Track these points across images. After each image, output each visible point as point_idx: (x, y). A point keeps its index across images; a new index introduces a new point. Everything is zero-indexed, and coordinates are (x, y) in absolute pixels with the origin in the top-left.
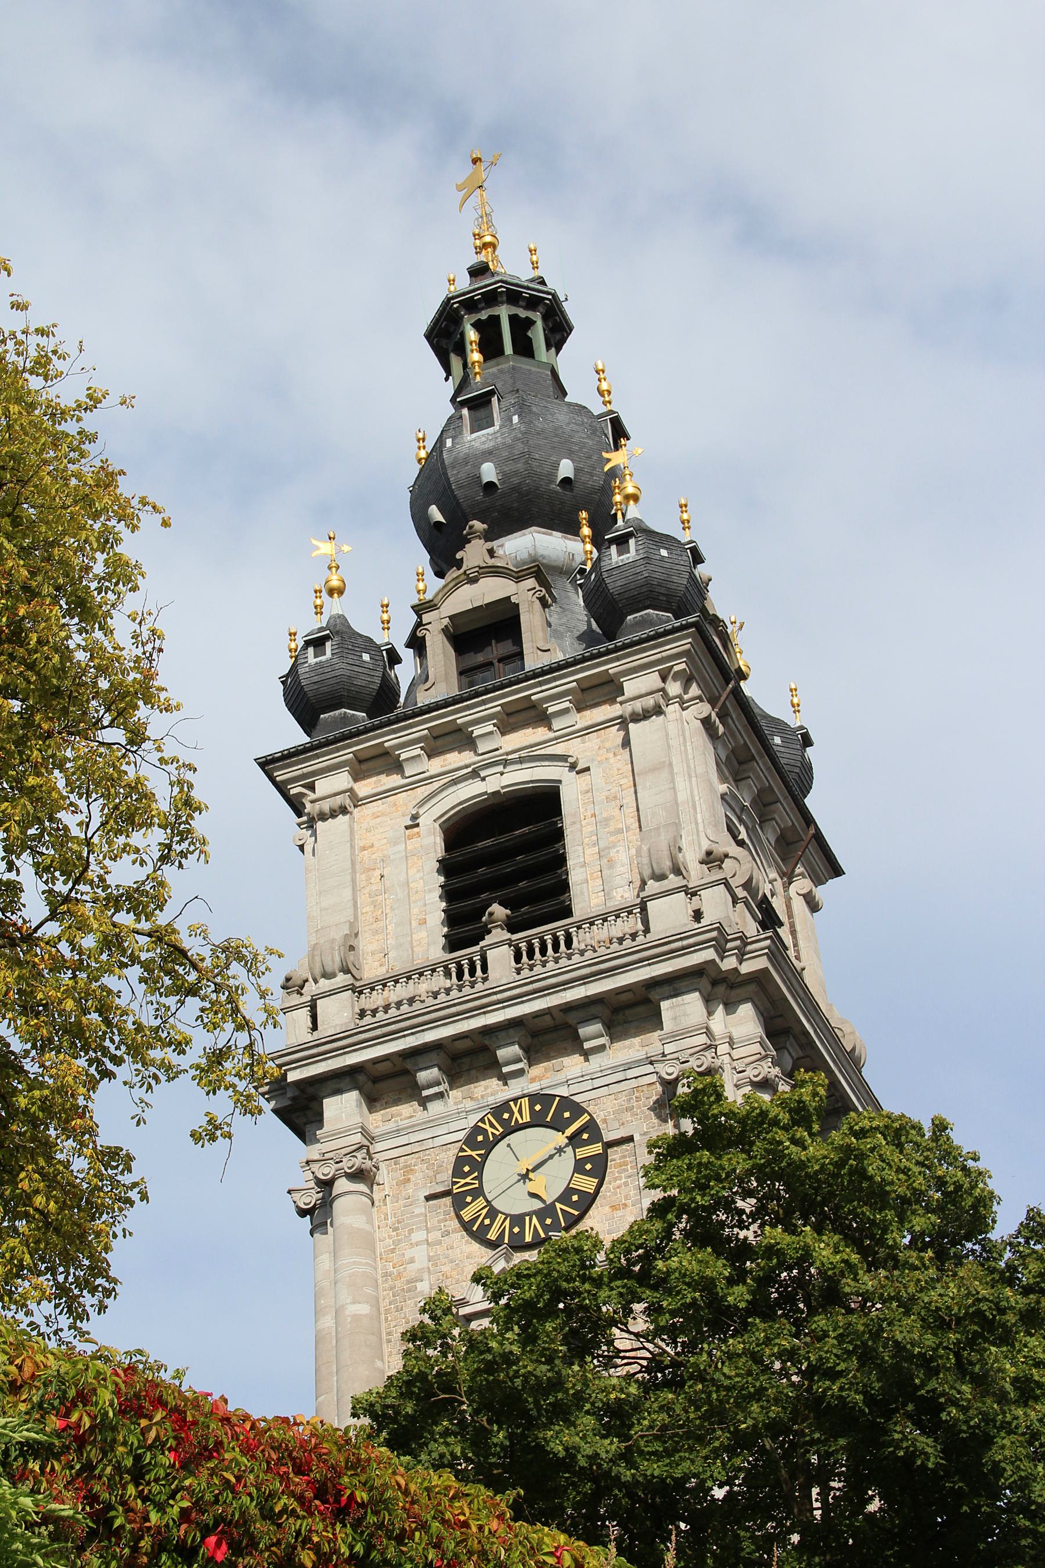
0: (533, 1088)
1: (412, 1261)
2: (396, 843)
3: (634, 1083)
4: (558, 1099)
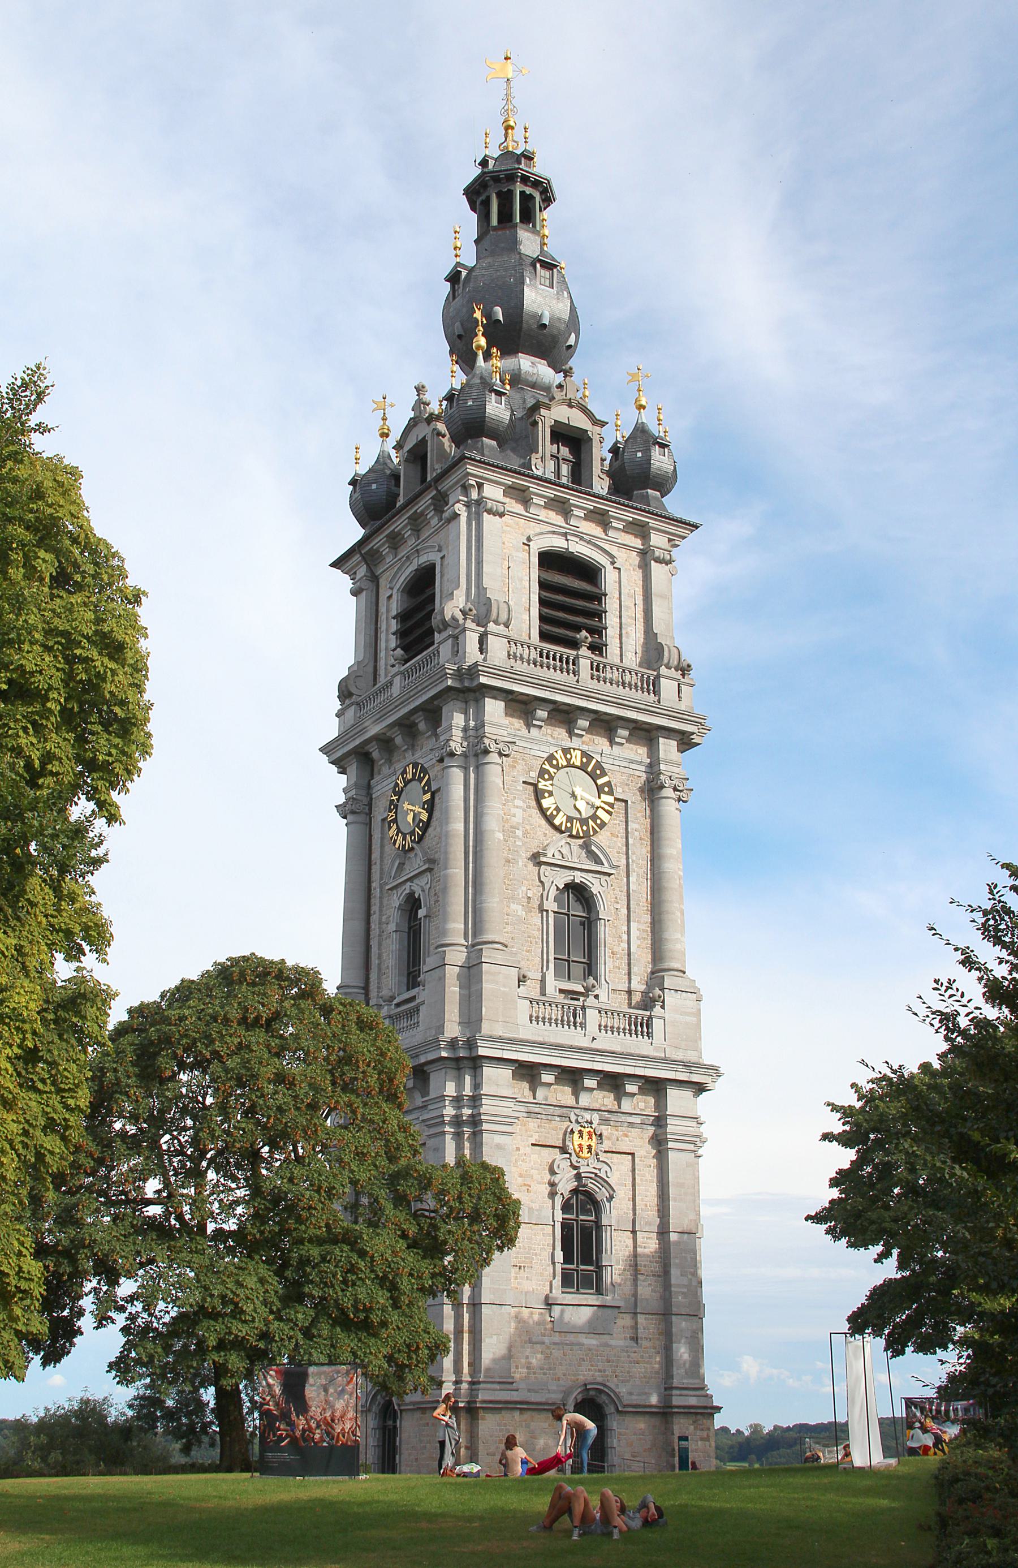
0: (585, 748)
1: (514, 816)
2: (517, 551)
3: (631, 772)
4: (594, 761)
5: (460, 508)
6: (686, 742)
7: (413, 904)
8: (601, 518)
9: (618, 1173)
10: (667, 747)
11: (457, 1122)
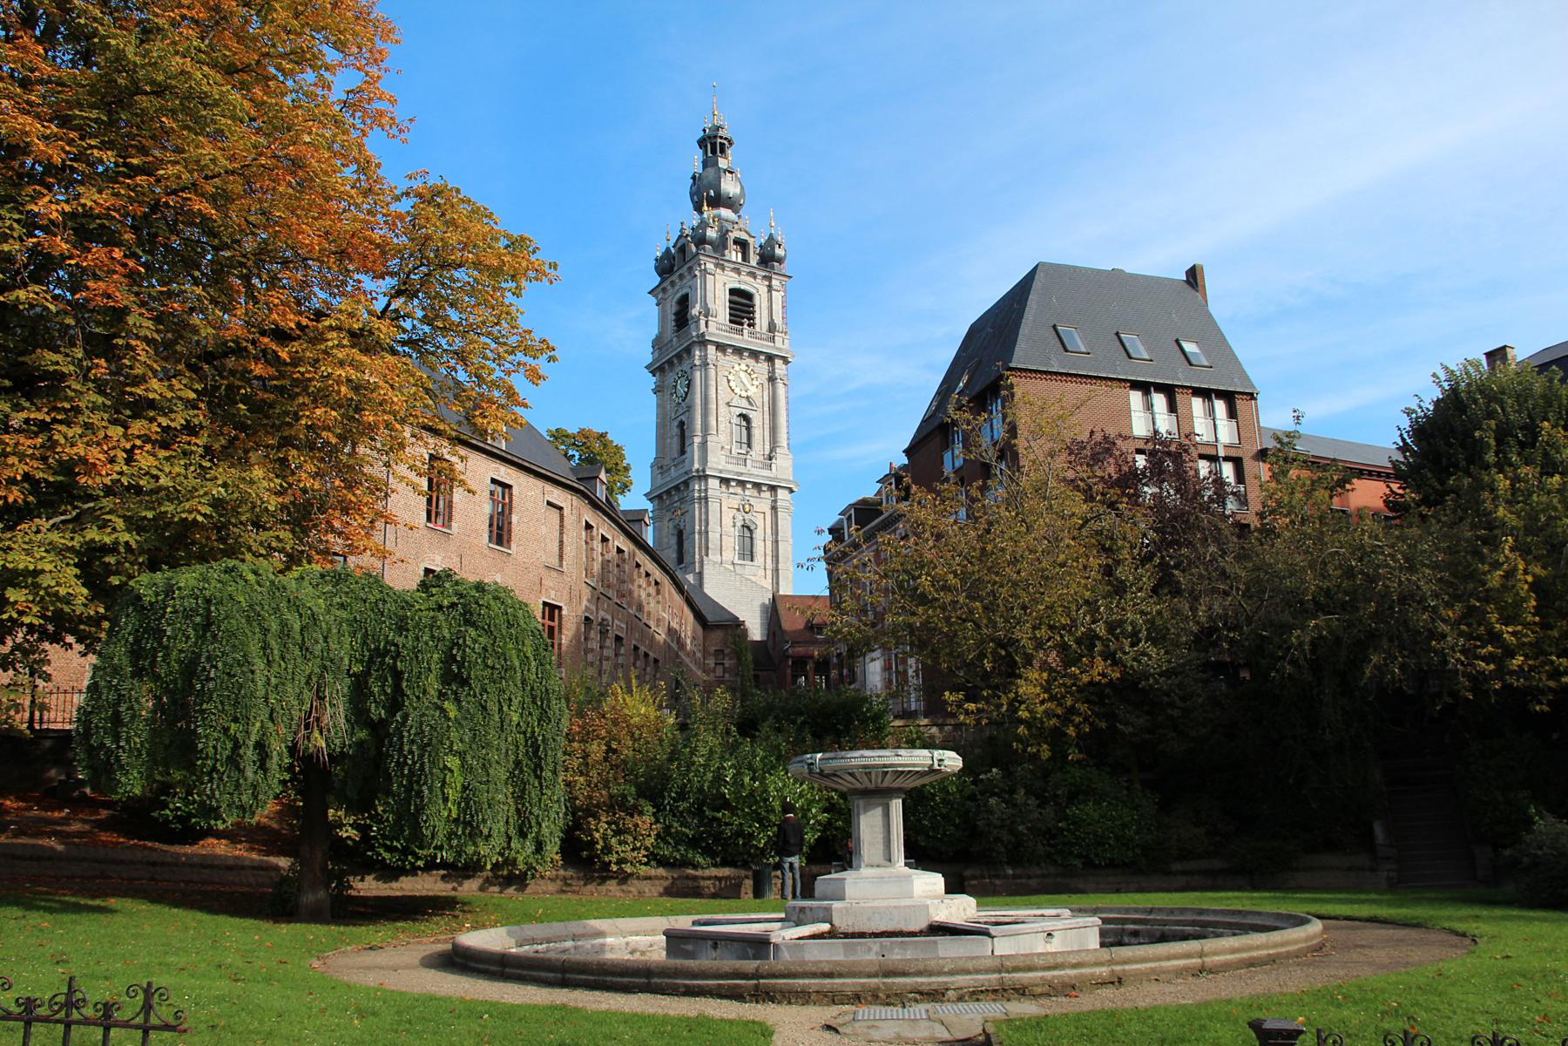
5: (697, 273)
6: (785, 360)
7: (682, 424)
8: (754, 275)
9: (759, 521)
10: (778, 363)
11: (700, 498)
